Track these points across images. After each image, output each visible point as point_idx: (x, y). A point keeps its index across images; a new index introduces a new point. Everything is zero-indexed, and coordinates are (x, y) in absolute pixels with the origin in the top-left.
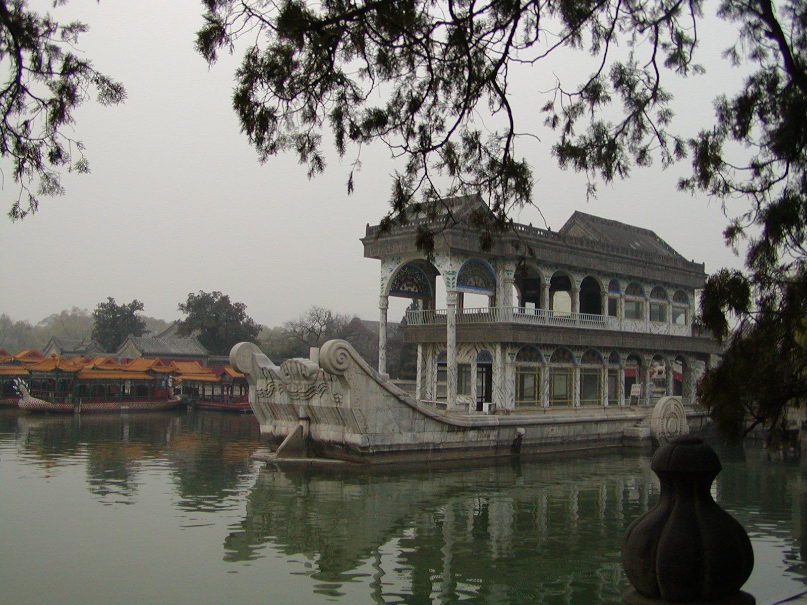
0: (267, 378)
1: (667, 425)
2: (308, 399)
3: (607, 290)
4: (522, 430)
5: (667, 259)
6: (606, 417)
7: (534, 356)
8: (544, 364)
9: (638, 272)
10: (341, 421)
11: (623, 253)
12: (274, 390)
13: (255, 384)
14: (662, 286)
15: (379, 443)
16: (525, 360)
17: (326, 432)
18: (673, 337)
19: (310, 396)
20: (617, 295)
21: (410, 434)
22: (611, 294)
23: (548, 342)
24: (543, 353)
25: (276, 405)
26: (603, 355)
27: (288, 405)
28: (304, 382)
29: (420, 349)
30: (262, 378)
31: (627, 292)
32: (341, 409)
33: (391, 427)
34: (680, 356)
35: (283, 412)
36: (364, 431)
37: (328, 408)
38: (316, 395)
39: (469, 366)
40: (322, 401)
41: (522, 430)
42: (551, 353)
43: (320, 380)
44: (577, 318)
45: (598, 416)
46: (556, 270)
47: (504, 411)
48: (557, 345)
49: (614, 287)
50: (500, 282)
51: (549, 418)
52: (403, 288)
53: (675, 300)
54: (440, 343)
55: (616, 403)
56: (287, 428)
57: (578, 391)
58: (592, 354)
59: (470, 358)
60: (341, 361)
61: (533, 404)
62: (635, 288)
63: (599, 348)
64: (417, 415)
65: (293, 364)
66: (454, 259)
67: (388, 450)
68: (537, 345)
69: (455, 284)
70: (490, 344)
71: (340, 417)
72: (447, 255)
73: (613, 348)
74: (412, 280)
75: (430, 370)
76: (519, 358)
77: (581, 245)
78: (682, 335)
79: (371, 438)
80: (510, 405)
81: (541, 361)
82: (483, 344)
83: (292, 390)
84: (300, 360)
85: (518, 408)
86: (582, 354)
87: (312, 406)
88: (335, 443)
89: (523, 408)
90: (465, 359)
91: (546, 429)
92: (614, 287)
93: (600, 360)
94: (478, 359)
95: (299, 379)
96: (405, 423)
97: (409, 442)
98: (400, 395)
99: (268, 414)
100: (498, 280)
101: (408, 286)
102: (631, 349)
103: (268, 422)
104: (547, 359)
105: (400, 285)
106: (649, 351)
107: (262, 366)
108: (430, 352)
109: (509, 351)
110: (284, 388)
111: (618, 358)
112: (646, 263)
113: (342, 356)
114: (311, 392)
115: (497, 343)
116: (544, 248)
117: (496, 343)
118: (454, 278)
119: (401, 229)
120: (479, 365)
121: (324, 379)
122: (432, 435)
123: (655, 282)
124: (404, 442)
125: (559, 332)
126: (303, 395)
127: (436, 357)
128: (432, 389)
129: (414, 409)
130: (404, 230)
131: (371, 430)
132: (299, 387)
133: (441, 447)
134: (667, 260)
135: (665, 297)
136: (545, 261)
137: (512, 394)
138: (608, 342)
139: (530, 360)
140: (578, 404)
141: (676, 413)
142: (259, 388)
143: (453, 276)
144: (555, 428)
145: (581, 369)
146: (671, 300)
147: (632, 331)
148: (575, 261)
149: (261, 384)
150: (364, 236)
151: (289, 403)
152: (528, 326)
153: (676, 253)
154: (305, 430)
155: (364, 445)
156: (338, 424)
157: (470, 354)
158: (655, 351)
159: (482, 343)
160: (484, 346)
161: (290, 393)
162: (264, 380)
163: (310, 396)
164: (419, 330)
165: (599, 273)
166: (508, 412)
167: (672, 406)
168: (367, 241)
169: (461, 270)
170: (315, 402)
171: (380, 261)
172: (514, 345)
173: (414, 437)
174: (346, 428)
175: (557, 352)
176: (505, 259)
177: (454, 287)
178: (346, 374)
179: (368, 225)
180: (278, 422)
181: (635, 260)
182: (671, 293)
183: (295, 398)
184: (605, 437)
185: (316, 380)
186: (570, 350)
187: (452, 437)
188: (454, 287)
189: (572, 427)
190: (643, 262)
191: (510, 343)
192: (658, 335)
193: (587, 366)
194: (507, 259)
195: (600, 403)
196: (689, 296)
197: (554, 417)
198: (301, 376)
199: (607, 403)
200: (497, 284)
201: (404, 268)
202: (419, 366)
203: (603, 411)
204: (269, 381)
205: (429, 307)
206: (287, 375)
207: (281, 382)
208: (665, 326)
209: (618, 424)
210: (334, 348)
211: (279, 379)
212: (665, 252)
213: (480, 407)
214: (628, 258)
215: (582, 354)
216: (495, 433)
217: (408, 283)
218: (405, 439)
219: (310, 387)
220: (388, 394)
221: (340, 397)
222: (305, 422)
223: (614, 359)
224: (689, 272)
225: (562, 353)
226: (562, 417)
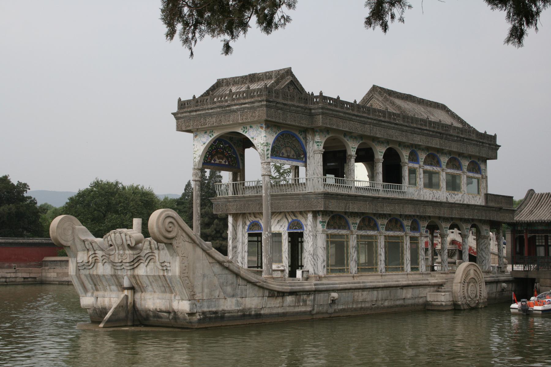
0: (88, 250)
2: (133, 269)
3: (407, 161)
4: (335, 295)
5: (462, 130)
6: (410, 282)
7: (343, 224)
8: (352, 232)
9: (435, 143)
10: (167, 289)
11: (421, 125)
12: (96, 262)
13: (76, 256)
14: (457, 157)
15: (206, 309)
16: (335, 228)
17: (152, 301)
18: (468, 206)
19: (135, 265)
20: (416, 166)
21: (234, 300)
22: (411, 165)
23: (356, 211)
25: (98, 276)
27: (111, 275)
28: (128, 252)
29: (230, 219)
30: (84, 250)
31: (425, 163)
32: (169, 277)
33: (217, 293)
34: (475, 225)
35: (105, 283)
36: (192, 298)
37: (154, 276)
38: (142, 265)
39: (279, 235)
40: (148, 270)
41: (335, 295)
43: (146, 249)
44: (380, 188)
45: (404, 282)
46: (361, 142)
47: (317, 277)
48: (363, 214)
49: (413, 158)
50: (310, 153)
51: (359, 283)
52: (215, 160)
53: (469, 170)
54: (250, 213)
55: (417, 269)
56: (111, 299)
57: (383, 258)
58: (395, 222)
59: (281, 227)
60: (170, 229)
61: (342, 271)
62: (433, 159)
63: (401, 216)
64: (240, 281)
65: (118, 234)
66: (268, 130)
67: (214, 315)
68: (346, 213)
69: (269, 156)
70: (301, 213)
71: (166, 285)
72: (262, 127)
73: (414, 216)
74: (222, 153)
75: (241, 240)
76: (329, 226)
77: (384, 117)
78: (476, 204)
79: (198, 305)
80: (322, 272)
81: (349, 229)
82: (294, 213)
83: (116, 261)
84: (125, 230)
85: (330, 275)
86: (386, 222)
87: (138, 276)
88: (161, 311)
89: (333, 275)
90: (276, 228)
92: (413, 158)
93: (401, 228)
94: (289, 228)
95: (124, 249)
96: (229, 289)
97: (234, 308)
98: (224, 262)
99: (89, 286)
100: (307, 151)
101: (219, 158)
102: (429, 217)
103: (89, 294)
105: (212, 158)
106: (446, 219)
107: (83, 238)
108: (240, 223)
109: (320, 219)
110: (108, 259)
111: (418, 224)
112: (443, 134)
113: (171, 225)
114: (135, 262)
115: (309, 211)
116: (351, 120)
117: (306, 212)
118: (268, 150)
119: (215, 103)
120: (290, 235)
121: (151, 248)
122: (253, 302)
123: (450, 153)
124: (229, 308)
125: (366, 201)
126: (128, 264)
127: (247, 227)
128: (243, 258)
129: (237, 275)
130: (218, 104)
131: (198, 296)
132: (124, 258)
133: (262, 312)
134: (462, 131)
135: (459, 167)
136: (351, 133)
137: (324, 261)
138: (409, 210)
139: (339, 228)
140: (384, 270)
141: (476, 278)
142: (79, 259)
143: (268, 147)
144: (365, 293)
145: (385, 236)
146: (465, 170)
147: (430, 200)
148: (379, 133)
149: (82, 257)
150: (175, 110)
151: (113, 273)
152: (337, 195)
153: (468, 125)
154: (130, 300)
155: (192, 311)
156: (165, 292)
157: (281, 224)
158: (452, 219)
159: (292, 212)
160: (295, 216)
161: (113, 264)
162: (86, 252)
163: (135, 265)
164: (229, 202)
165: (400, 144)
166: (320, 278)
167: (472, 272)
168: (179, 115)
169: (274, 142)
170: (142, 271)
171: (191, 135)
172: (325, 213)
173: (238, 303)
174: (173, 295)
175: (363, 220)
176: (314, 131)
177: (268, 158)
178: (174, 242)
179: (180, 100)
180: (100, 293)
181: (433, 132)
182: (465, 163)
183: (119, 268)
185: (141, 250)
187: (272, 302)
188: (268, 158)
189: (380, 292)
190: (440, 133)
191: (321, 211)
192: (455, 204)
193: (391, 233)
194: (317, 132)
196: (482, 166)
197: (363, 282)
198: (126, 247)
199: (409, 269)
200: (308, 155)
201: (215, 142)
202: (230, 236)
203: (406, 276)
204: (91, 253)
205: (239, 179)
206: (111, 245)
207: (104, 254)
208: (460, 195)
209: (421, 289)
210: (164, 215)
211: (102, 250)
212: (460, 126)
213: (292, 274)
214: (426, 130)
215: (386, 222)
216: (312, 297)
217: (219, 155)
218: (229, 305)
219: (135, 256)
220: (214, 261)
221: (168, 265)
222: (130, 291)
223: (415, 228)
224: (483, 143)
225: (368, 221)
226: (371, 282)
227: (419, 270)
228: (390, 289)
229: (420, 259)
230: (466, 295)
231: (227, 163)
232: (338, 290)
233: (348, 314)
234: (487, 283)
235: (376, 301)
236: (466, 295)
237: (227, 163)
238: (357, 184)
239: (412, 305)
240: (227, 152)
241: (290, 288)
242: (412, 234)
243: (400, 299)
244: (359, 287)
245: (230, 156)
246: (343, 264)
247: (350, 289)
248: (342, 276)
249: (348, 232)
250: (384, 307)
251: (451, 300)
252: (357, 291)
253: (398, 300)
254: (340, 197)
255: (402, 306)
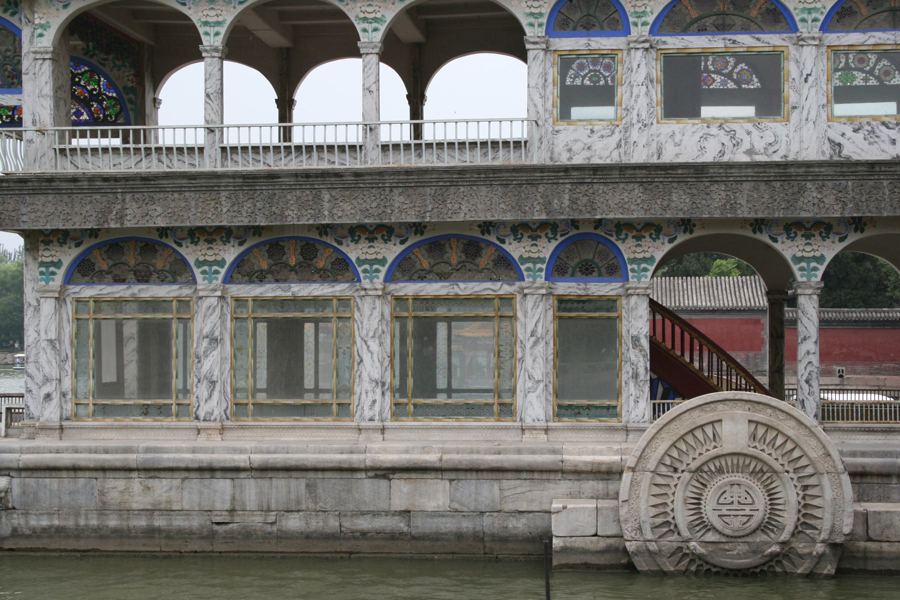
1: (697, 503)
24: (191, 253)
26: (515, 249)
42: (230, 253)
55: (612, 411)
61: (163, 411)
68: (163, 232)
81: (194, 281)
86: (391, 251)
89: (109, 421)
91: (121, 484)
93: (506, 266)
104: (209, 276)
139: (143, 278)
184: (448, 525)
186: (330, 240)
195: (507, 410)
197: (148, 450)
209: (510, 484)
215: (391, 251)
226: (194, 451)
227: (617, 415)
228: (311, 475)
229: (624, 377)
230: (682, 517)
231: (85, 117)
232: (9, 469)
233: (82, 545)
234: (853, 475)
235: (232, 511)
236: (682, 517)
237: (85, 117)
238: (232, 138)
239: (459, 536)
240: (85, 87)
241: (189, 456)
242: (567, 287)
243: (375, 514)
244: (118, 464)
245: (98, 97)
246: (164, 389)
247: (75, 469)
248: (152, 428)
249: (186, 291)
250: (284, 536)
251: (612, 530)
252: (122, 474)
253: (363, 514)
254: (64, 185)
255: (394, 536)
